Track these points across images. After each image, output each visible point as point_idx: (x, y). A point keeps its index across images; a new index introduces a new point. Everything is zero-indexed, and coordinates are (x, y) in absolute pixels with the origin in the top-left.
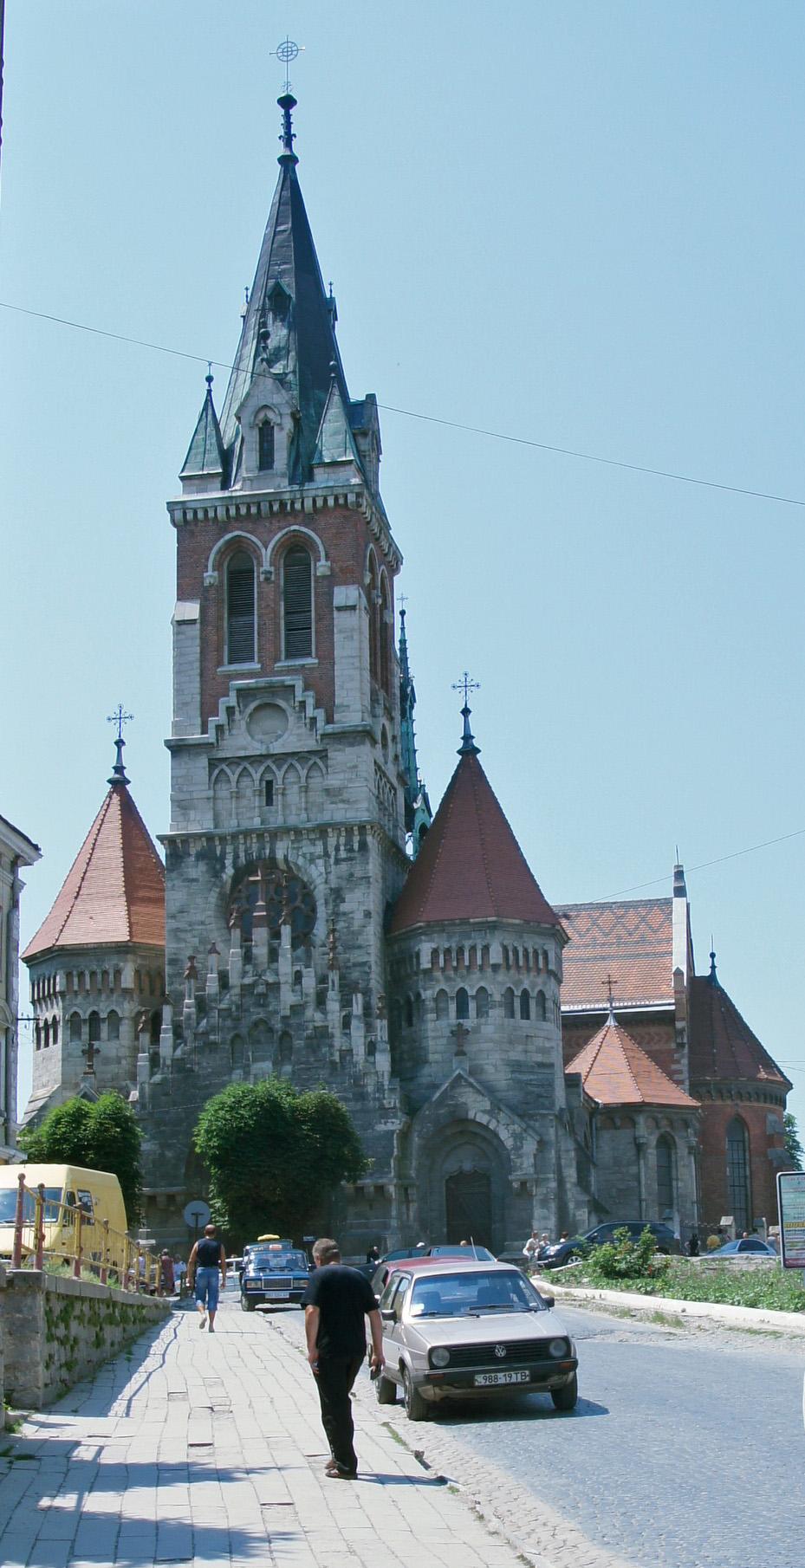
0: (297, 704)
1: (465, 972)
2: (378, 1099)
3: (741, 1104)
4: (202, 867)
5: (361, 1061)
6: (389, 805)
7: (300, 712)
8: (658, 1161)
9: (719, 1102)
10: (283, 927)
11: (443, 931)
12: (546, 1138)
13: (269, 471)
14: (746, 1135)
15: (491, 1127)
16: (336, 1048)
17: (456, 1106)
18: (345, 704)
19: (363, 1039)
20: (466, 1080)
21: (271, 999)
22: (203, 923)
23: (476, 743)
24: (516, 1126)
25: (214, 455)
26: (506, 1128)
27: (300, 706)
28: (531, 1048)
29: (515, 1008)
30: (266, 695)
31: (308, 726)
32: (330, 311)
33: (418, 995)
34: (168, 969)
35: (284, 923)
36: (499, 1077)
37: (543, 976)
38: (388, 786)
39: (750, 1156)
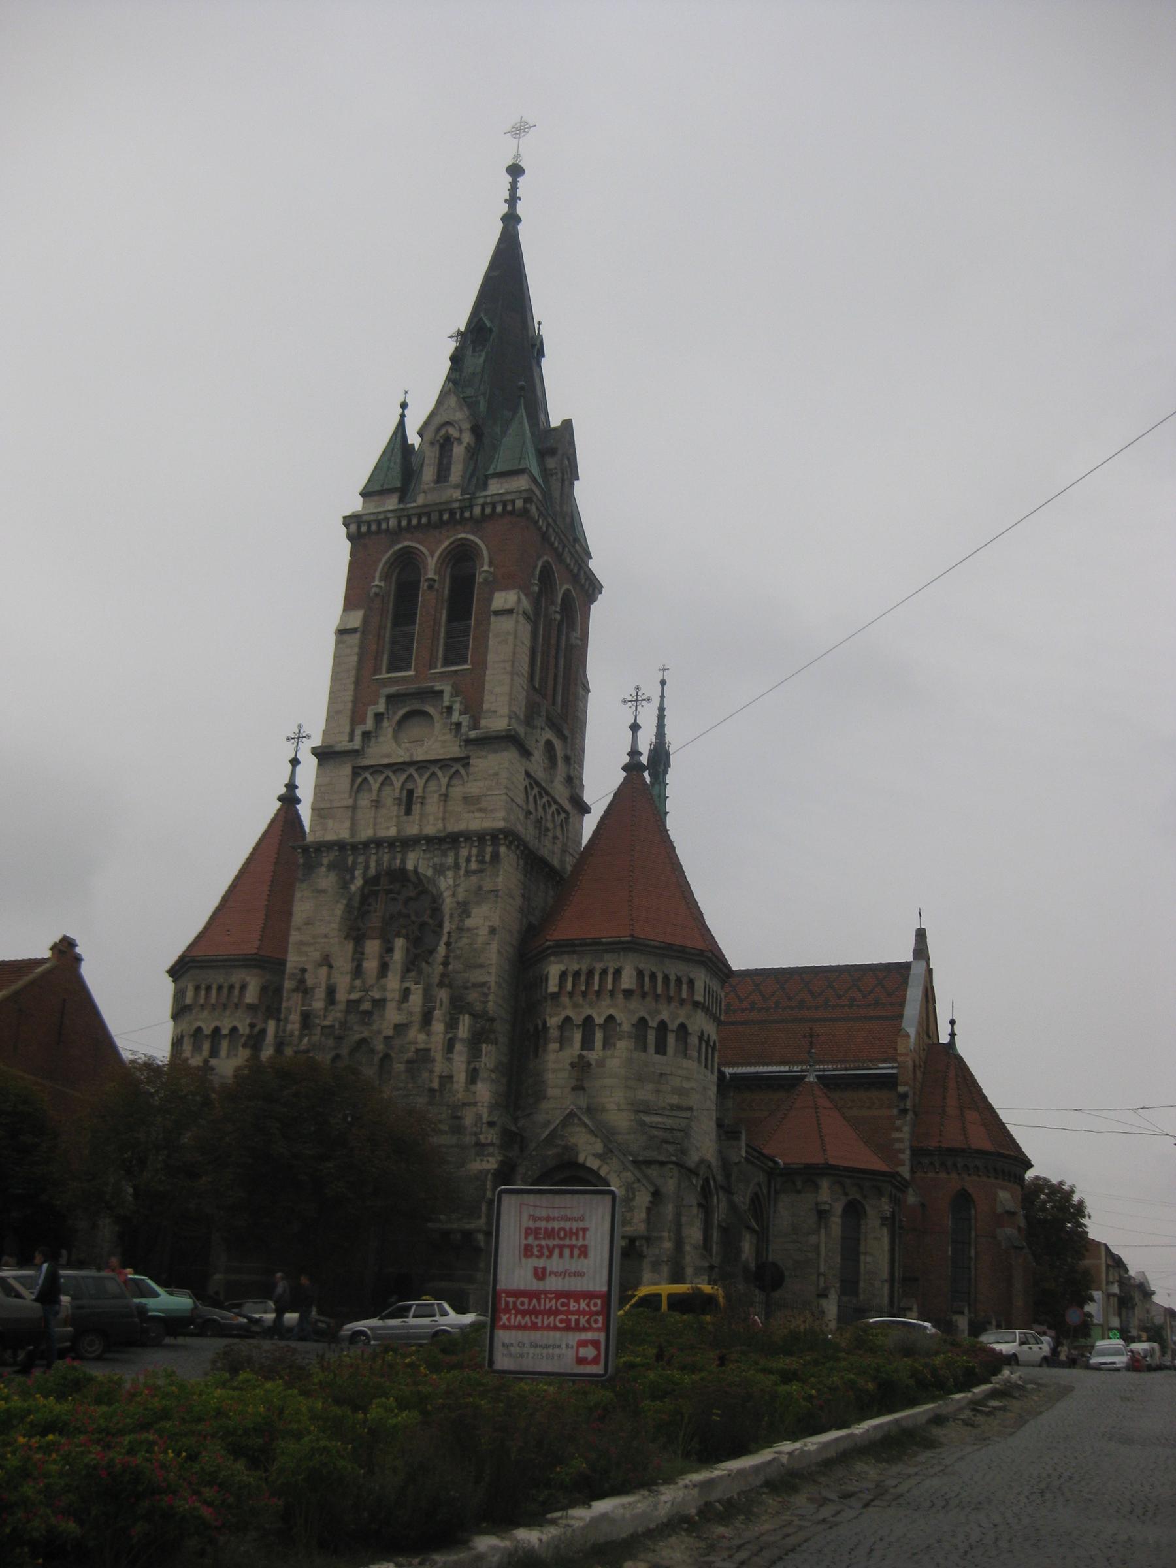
0: (444, 710)
1: (594, 998)
2: (476, 1134)
5: (461, 1089)
6: (555, 828)
7: (446, 718)
9: (943, 1175)
10: (397, 940)
11: (574, 952)
13: (446, 484)
14: (973, 1212)
15: (603, 1173)
16: (436, 1074)
17: (566, 1148)
18: (493, 709)
19: (463, 1067)
20: (580, 1119)
22: (326, 936)
24: (629, 1174)
25: (397, 470)
26: (619, 1176)
27: (447, 712)
31: (453, 732)
32: (533, 346)
33: (545, 1023)
34: (288, 984)
35: (398, 935)
36: (620, 1119)
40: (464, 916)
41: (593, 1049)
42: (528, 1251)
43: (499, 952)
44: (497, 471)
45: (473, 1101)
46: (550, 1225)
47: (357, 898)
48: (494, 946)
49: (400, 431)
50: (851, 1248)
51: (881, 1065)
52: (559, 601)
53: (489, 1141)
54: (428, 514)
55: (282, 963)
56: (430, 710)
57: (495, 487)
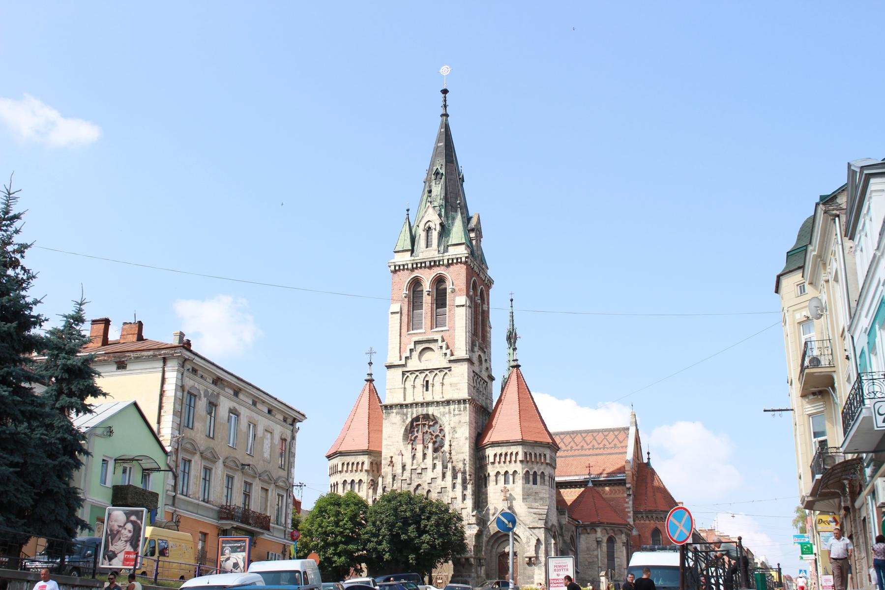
2: (468, 520)
4: (398, 417)
6: (483, 390)
8: (607, 549)
9: (647, 522)
11: (499, 446)
12: (540, 539)
14: (661, 537)
18: (459, 347)
21: (423, 475)
23: (519, 363)
28: (537, 498)
31: (444, 356)
34: (383, 462)
37: (544, 465)
38: (482, 381)
41: (509, 484)
42: (555, 570)
43: (469, 447)
44: (453, 243)
46: (560, 564)
47: (409, 426)
49: (407, 222)
50: (611, 556)
51: (619, 475)
52: (479, 294)
54: (425, 262)
55: (379, 453)
57: (453, 252)
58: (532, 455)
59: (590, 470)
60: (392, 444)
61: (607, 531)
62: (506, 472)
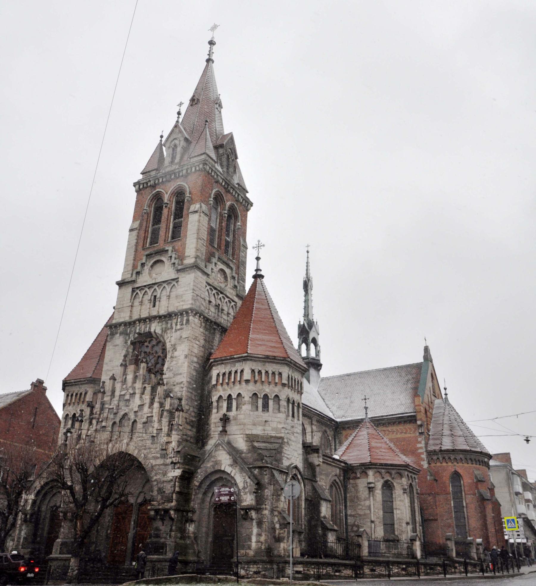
2: (171, 458)
3: (458, 465)
6: (228, 309)
9: (444, 464)
12: (262, 482)
14: (462, 482)
15: (232, 475)
19: (167, 424)
21: (131, 402)
29: (259, 405)
30: (158, 256)
37: (279, 387)
39: (465, 495)
40: (174, 350)
43: (189, 366)
45: (170, 441)
48: (186, 364)
52: (227, 208)
53: (177, 461)
56: (163, 259)
58: (261, 373)
59: (366, 403)
60: (112, 369)
61: (381, 474)
62: (230, 396)
